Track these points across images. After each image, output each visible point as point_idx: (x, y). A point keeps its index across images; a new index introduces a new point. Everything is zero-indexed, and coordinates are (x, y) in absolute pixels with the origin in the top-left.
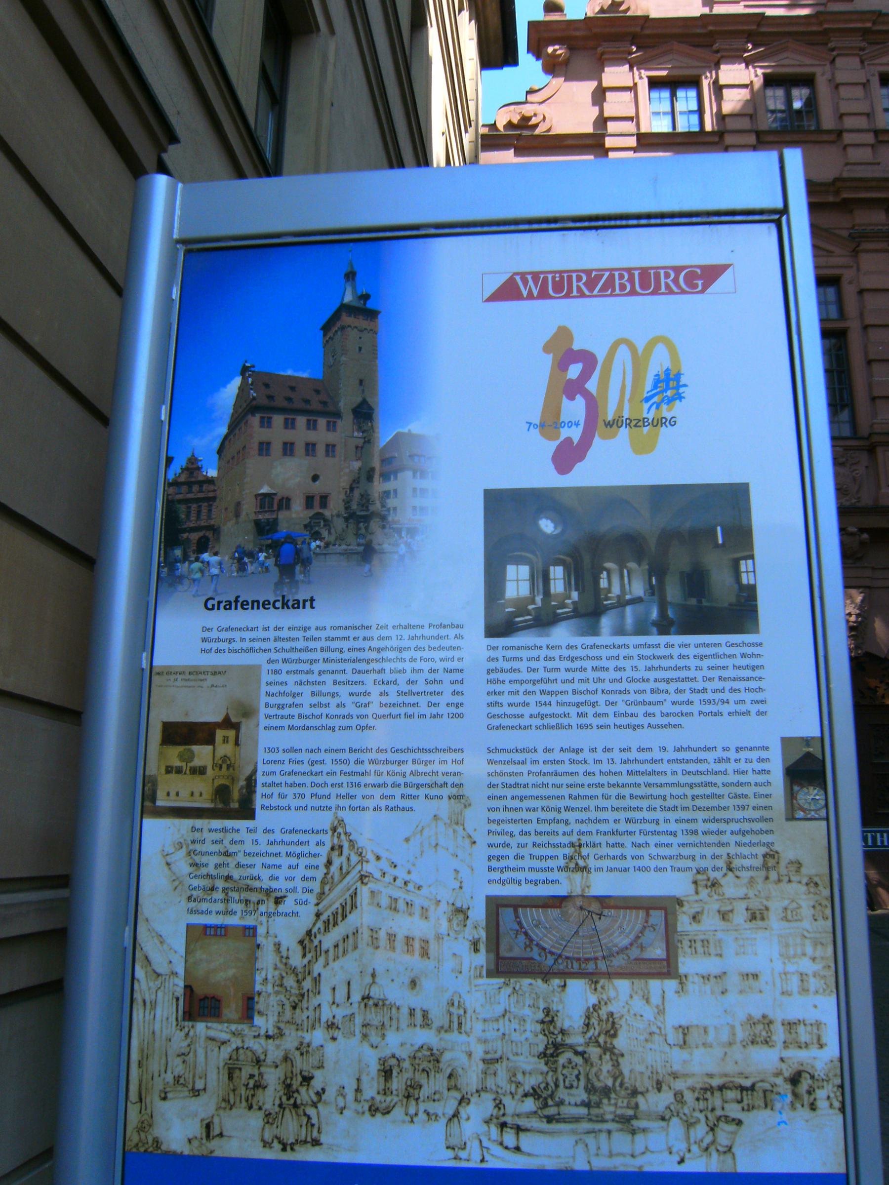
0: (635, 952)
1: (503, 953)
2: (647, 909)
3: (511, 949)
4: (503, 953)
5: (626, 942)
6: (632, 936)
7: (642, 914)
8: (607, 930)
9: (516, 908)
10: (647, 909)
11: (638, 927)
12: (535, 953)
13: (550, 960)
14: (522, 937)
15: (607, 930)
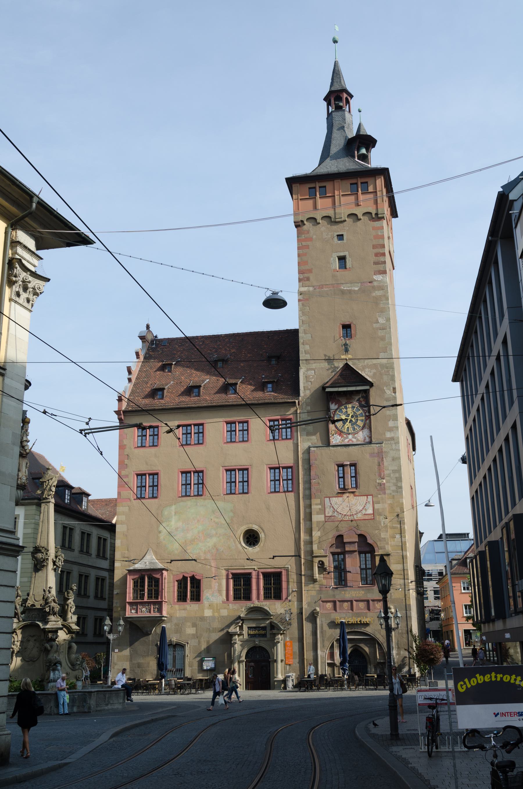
0: (364, 512)
1: (327, 515)
2: (367, 496)
3: (329, 513)
4: (327, 515)
5: (361, 508)
6: (363, 506)
7: (366, 497)
8: (356, 504)
9: (329, 497)
10: (367, 496)
11: (365, 503)
12: (335, 514)
13: (340, 516)
14: (332, 508)
15: (356, 504)
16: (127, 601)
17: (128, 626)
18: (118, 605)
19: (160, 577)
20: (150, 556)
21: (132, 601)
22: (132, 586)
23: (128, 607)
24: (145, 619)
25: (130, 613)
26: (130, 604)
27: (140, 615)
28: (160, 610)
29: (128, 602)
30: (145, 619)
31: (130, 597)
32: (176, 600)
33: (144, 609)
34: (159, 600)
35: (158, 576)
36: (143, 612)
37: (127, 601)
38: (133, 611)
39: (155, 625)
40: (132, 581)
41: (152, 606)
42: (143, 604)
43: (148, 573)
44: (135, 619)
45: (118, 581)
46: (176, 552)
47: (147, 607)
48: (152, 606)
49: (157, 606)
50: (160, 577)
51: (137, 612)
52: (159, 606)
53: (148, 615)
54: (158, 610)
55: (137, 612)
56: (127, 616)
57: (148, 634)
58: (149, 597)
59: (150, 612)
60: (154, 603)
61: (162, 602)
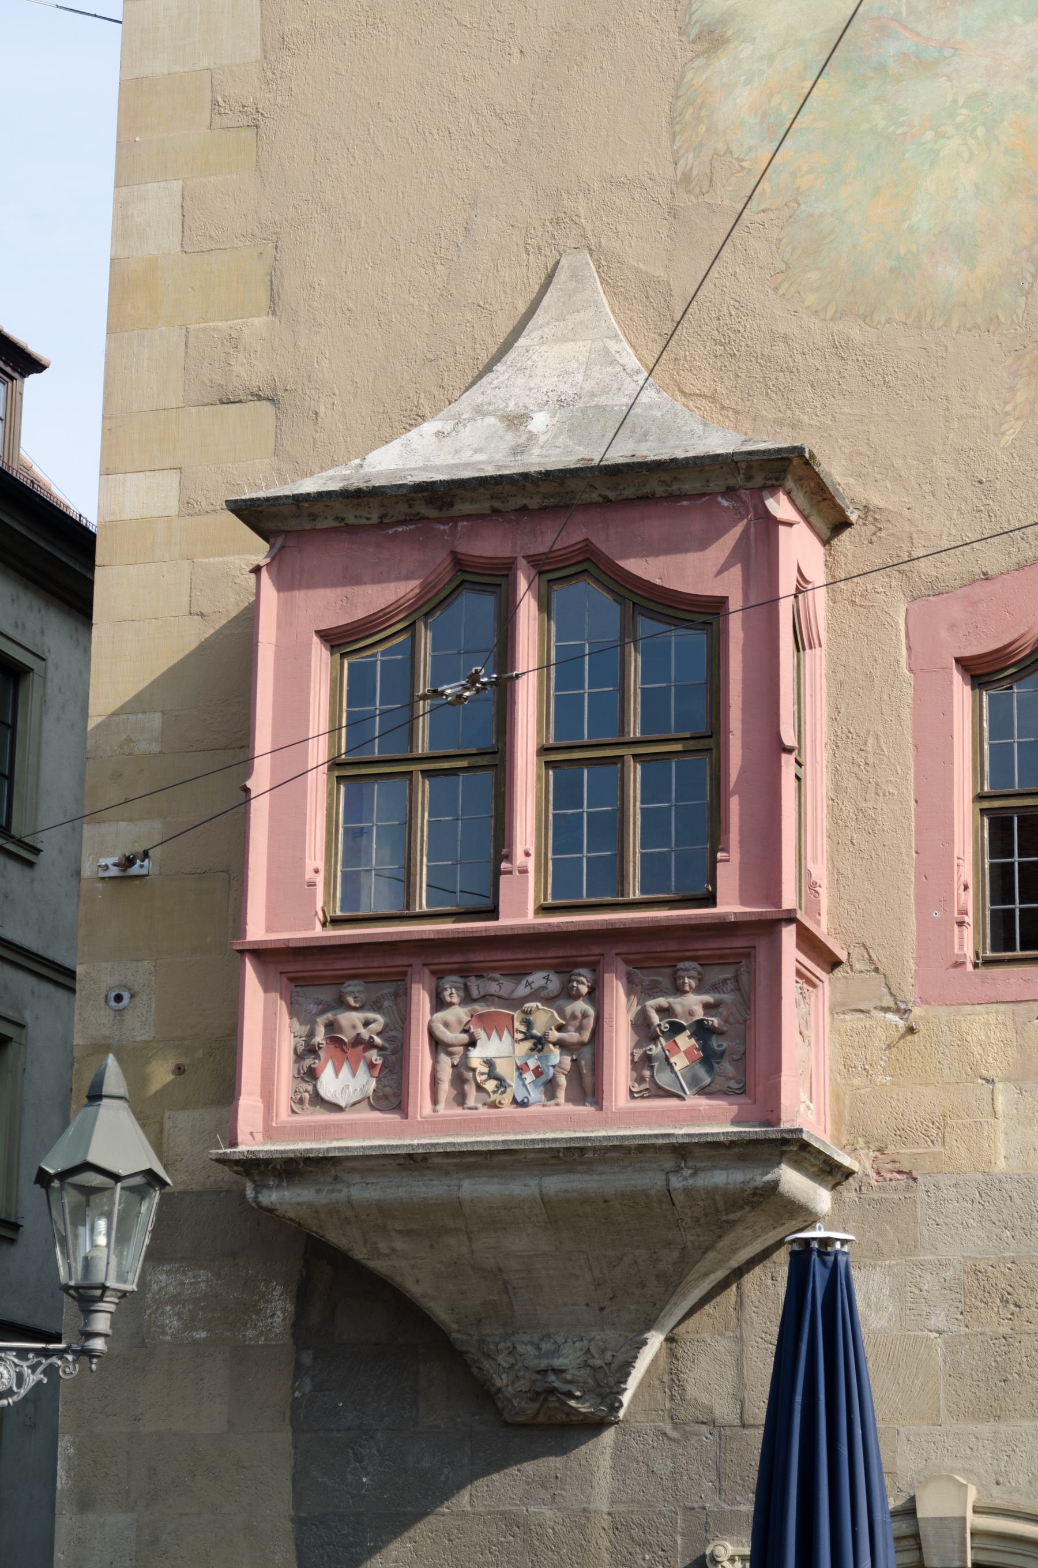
16: (258, 929)
17: (278, 1312)
18: (139, 1027)
19: (730, 586)
20: (579, 349)
21: (317, 932)
22: (319, 719)
23: (265, 1024)
24: (523, 1188)
25: (291, 1094)
26: (304, 971)
27: (433, 1121)
28: (740, 1053)
29: (262, 954)
30: (523, 1188)
31: (294, 867)
32: (967, 943)
33: (495, 1048)
34: (729, 905)
35: (697, 570)
36: (489, 1084)
37: (258, 929)
38: (339, 1082)
39: (671, 1285)
40: (320, 656)
41: (621, 1007)
42: (480, 962)
43: (547, 538)
44: (363, 1192)
45: (139, 703)
46: (951, 276)
47: (543, 1017)
48: (621, 1007)
49: (692, 1004)
50: (730, 586)
51: (392, 1096)
52: (724, 967)
53: (560, 1122)
54: (709, 1059)
55: (392, 1096)
56: (252, 1139)
57: (558, 1420)
58: (563, 877)
59: (588, 1087)
60: (653, 957)
61: (769, 928)
